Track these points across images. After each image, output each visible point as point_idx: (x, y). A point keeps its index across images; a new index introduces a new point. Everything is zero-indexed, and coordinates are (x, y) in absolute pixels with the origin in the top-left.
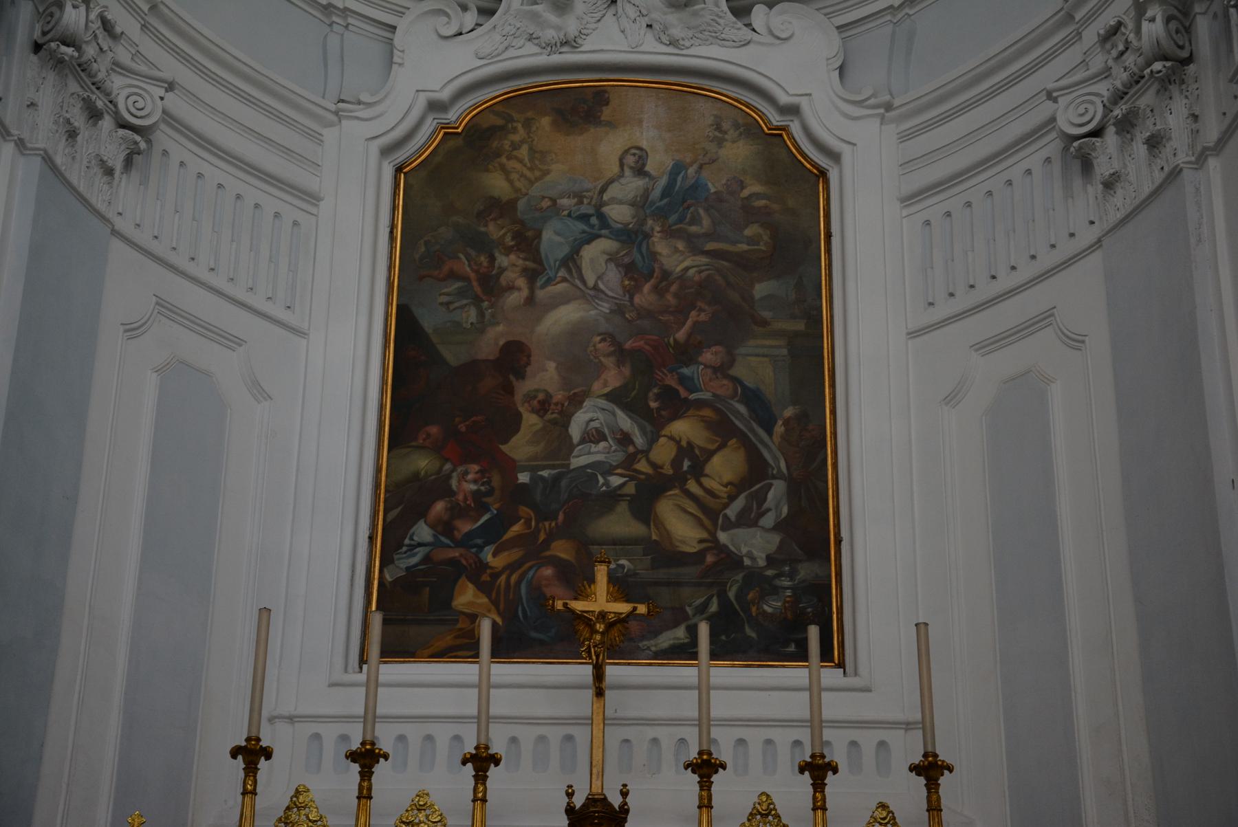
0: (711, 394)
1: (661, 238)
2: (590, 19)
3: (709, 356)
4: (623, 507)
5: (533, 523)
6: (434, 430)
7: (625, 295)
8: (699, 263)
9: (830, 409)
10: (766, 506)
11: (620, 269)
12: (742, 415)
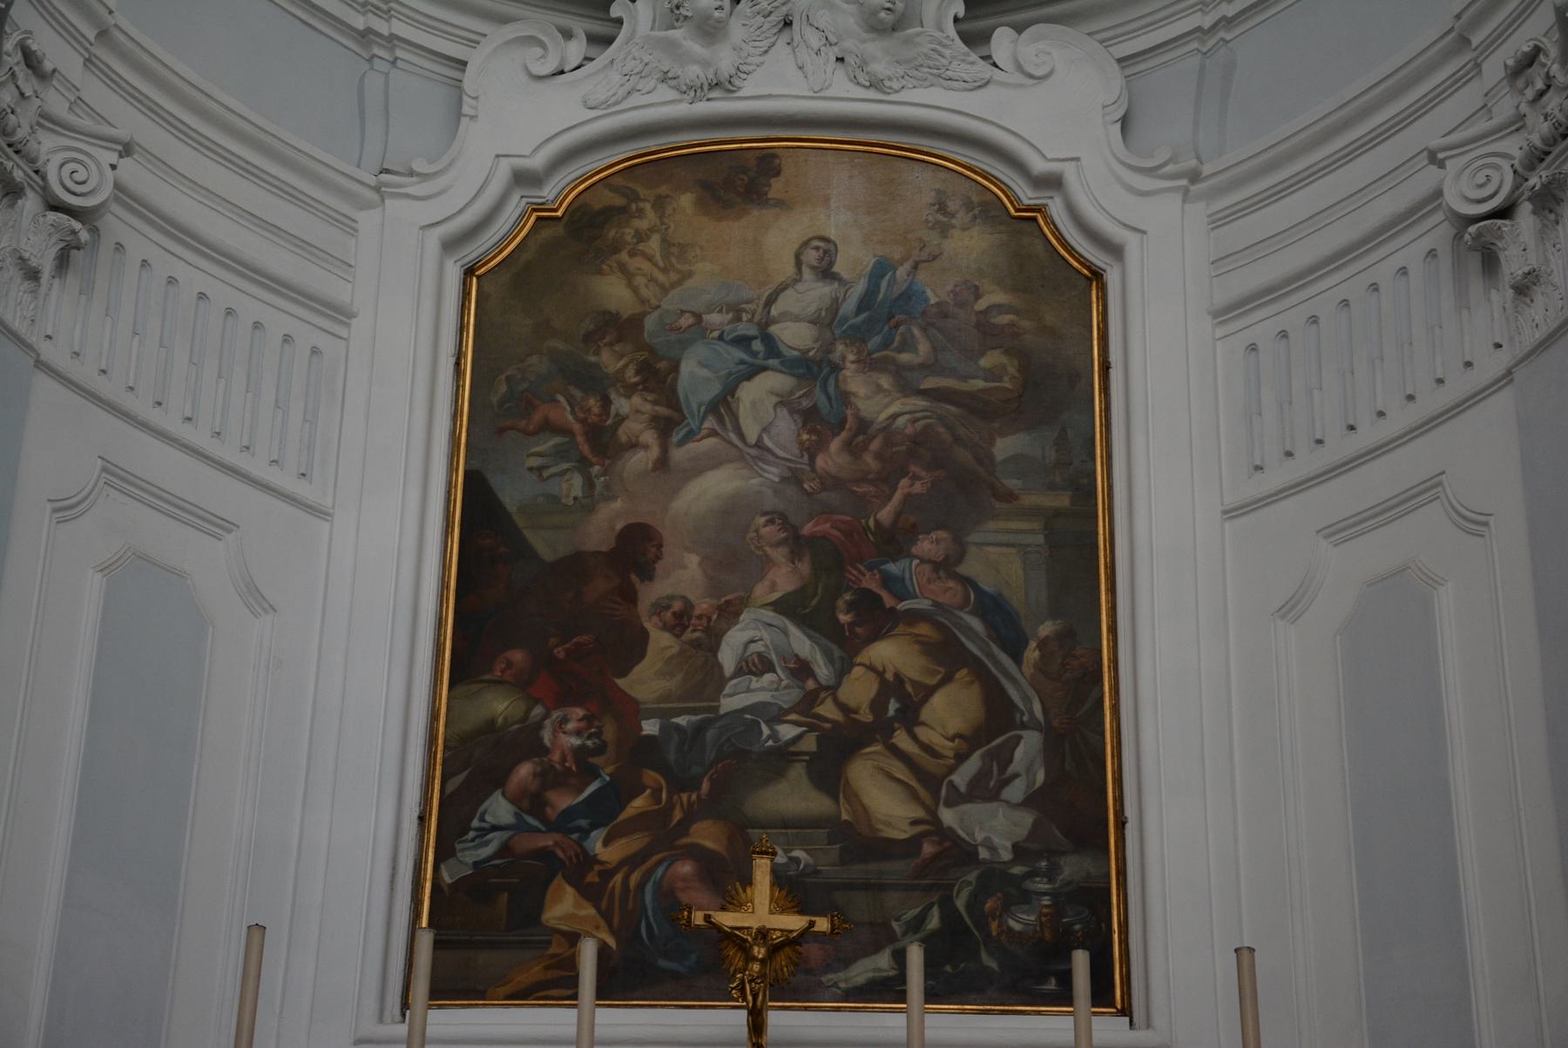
0: (931, 603)
1: (857, 371)
2: (752, 51)
3: (928, 546)
4: (798, 771)
5: (664, 796)
6: (517, 656)
7: (802, 456)
8: (912, 408)
9: (1108, 624)
10: (1011, 769)
11: (796, 416)
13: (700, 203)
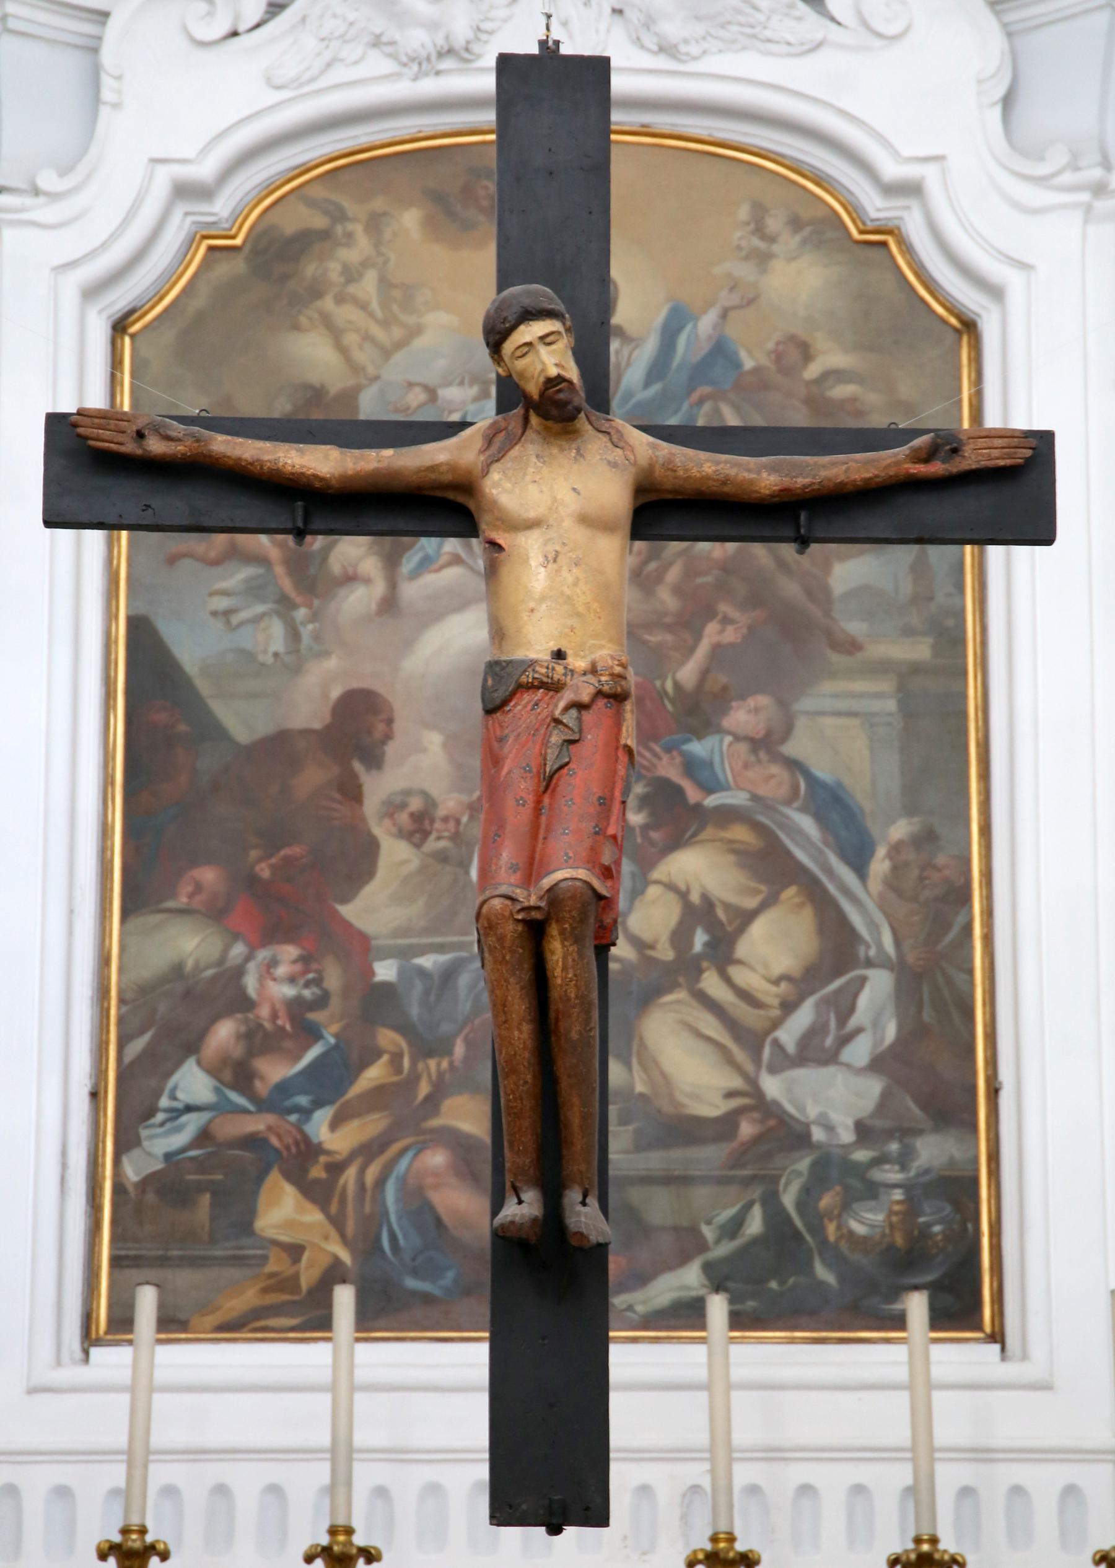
5: (406, 1063)
6: (208, 875)
10: (853, 1022)
12: (807, 838)
13: (430, 224)
